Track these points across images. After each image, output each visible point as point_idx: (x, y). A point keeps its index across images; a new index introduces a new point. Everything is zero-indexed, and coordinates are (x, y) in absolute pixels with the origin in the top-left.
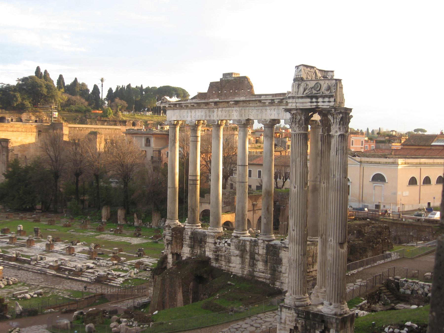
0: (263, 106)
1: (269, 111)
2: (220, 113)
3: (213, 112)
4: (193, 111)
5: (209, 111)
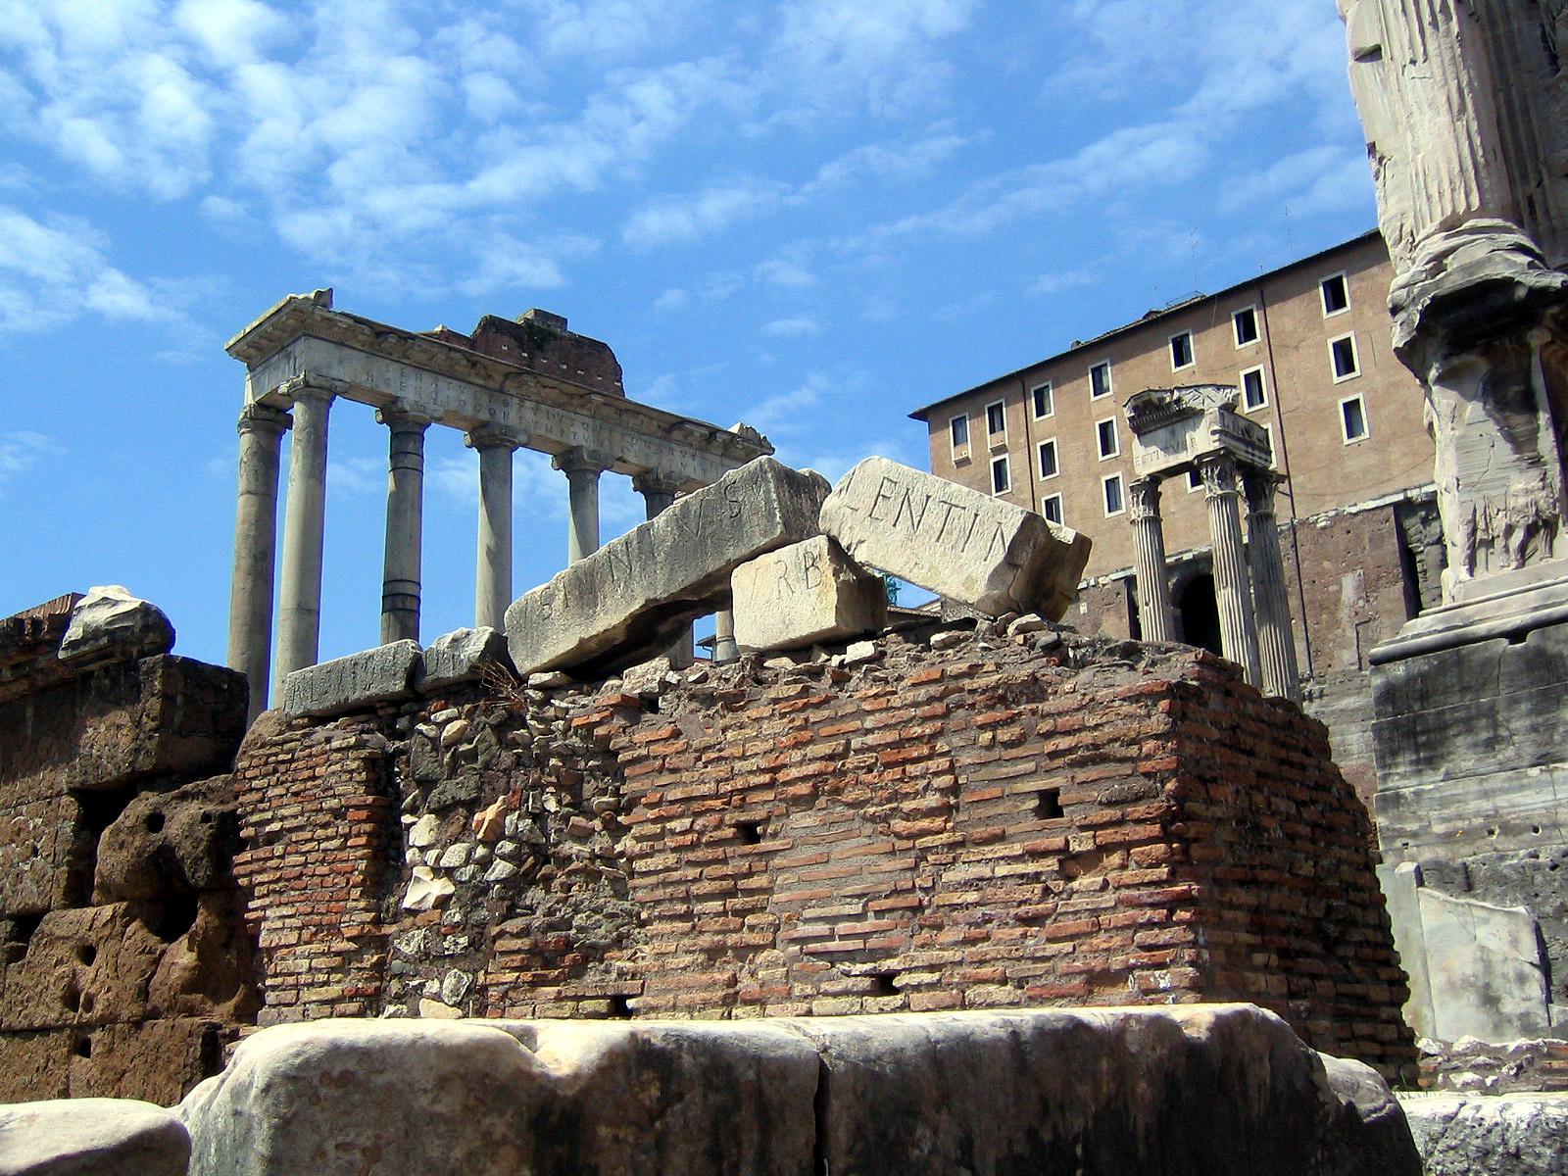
0: (665, 439)
1: (677, 454)
2: (529, 415)
3: (506, 404)
4: (427, 379)
5: (491, 397)
